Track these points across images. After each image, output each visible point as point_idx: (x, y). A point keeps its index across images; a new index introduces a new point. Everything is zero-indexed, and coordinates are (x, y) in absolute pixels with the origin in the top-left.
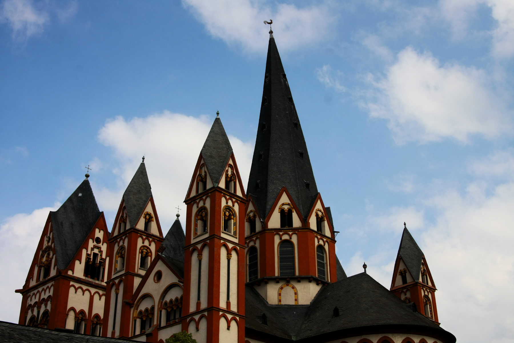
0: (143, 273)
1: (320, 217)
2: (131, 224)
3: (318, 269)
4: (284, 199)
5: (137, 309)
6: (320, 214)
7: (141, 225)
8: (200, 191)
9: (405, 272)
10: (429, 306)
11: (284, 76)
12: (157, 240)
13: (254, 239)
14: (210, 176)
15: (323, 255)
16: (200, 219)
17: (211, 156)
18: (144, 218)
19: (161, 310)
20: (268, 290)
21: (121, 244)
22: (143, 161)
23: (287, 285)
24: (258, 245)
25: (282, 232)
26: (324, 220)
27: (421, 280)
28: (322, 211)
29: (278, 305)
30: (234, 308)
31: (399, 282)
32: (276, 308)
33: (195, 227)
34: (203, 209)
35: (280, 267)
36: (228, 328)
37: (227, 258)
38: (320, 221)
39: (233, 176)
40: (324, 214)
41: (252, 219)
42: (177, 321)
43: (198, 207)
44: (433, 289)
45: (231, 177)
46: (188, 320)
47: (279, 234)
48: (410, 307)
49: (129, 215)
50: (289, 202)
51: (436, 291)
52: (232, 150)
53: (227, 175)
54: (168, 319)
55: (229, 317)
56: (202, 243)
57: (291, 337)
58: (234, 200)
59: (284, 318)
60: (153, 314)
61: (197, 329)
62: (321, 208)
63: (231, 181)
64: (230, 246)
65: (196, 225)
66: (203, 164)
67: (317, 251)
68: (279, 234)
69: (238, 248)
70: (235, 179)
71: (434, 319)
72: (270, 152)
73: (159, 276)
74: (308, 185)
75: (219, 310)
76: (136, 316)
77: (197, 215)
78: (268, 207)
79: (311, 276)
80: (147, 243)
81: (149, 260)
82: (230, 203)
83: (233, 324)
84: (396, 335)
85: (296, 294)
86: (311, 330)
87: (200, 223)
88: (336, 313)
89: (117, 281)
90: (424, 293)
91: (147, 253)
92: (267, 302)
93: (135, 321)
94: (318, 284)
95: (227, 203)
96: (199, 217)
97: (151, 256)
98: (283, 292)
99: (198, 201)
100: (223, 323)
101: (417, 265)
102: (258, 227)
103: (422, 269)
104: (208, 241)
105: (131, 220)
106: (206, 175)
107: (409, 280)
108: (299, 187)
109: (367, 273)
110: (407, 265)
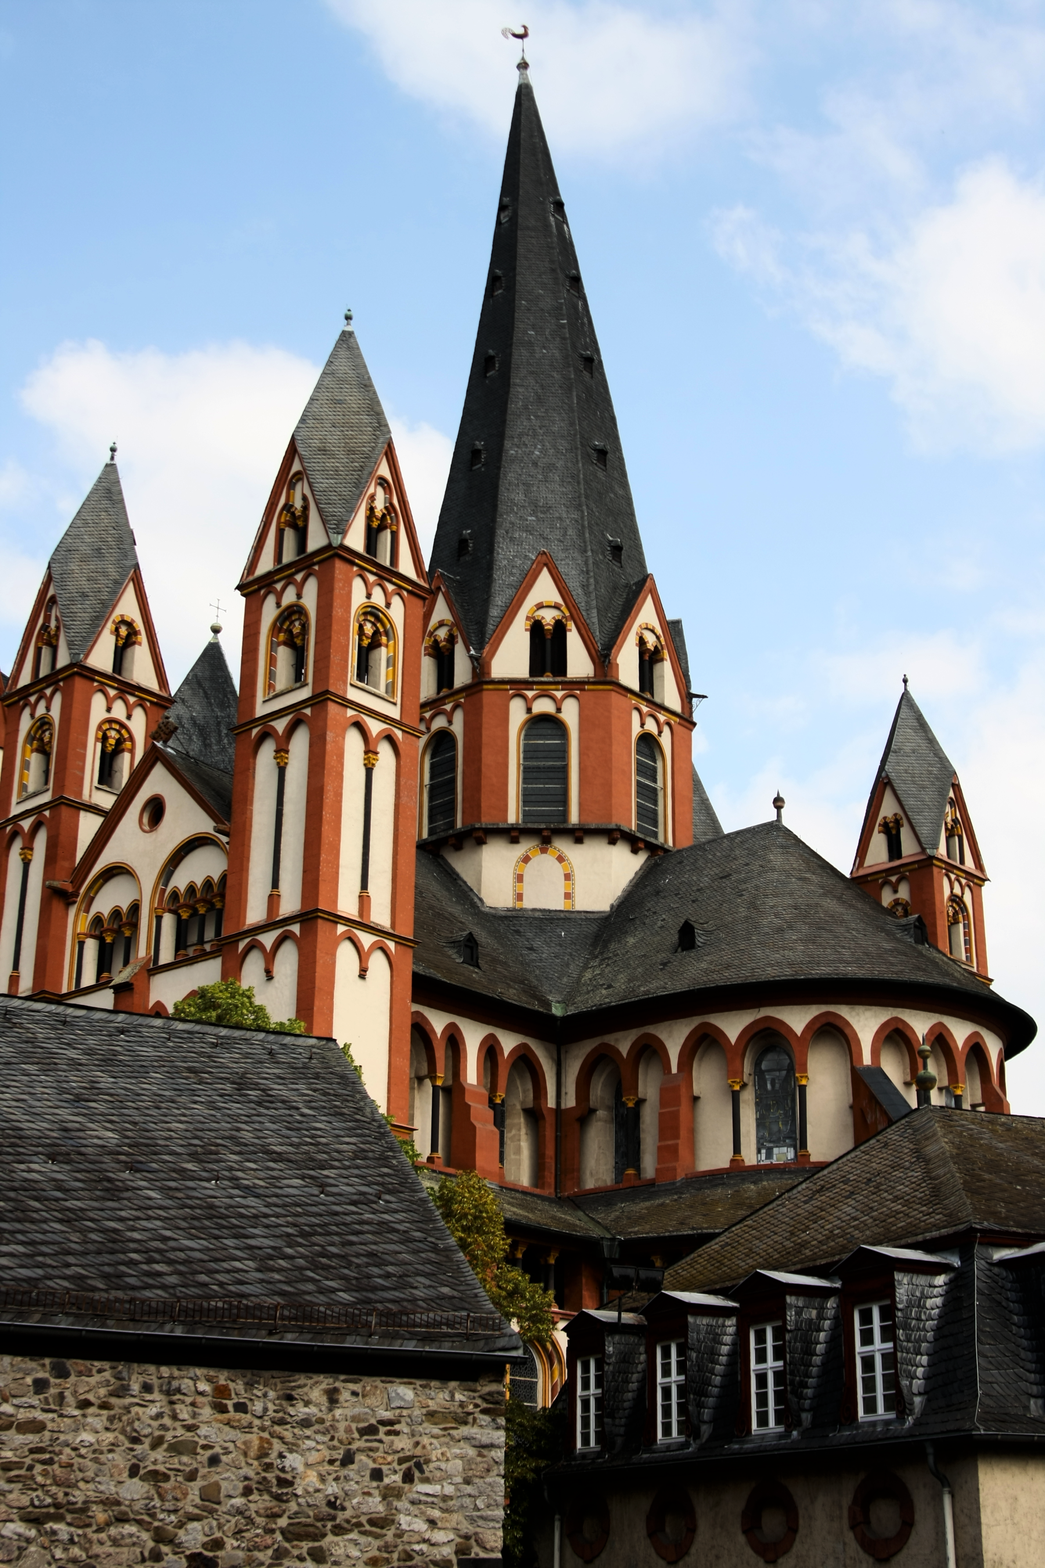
0: (106, 801)
1: (649, 650)
2: (73, 651)
5: (87, 911)
6: (651, 640)
7: (101, 658)
8: (288, 556)
9: (898, 823)
10: (964, 928)
11: (559, 206)
12: (151, 702)
13: (448, 707)
14: (320, 511)
15: (655, 763)
16: (285, 643)
17: (323, 450)
18: (112, 633)
19: (160, 914)
20: (484, 864)
21: (41, 710)
22: (112, 458)
23: (544, 851)
24: (457, 728)
25: (532, 689)
26: (662, 660)
27: (942, 850)
28: (659, 630)
29: (514, 909)
30: (381, 915)
31: (878, 854)
32: (506, 917)
33: (270, 666)
34: (294, 612)
35: (524, 795)
36: (362, 975)
37: (365, 765)
38: (648, 660)
39: (389, 514)
40: (662, 639)
41: (444, 646)
42: (207, 947)
43: (278, 605)
44: (977, 880)
45: (384, 515)
46: (242, 945)
47: (524, 697)
48: (906, 930)
49: (67, 623)
50: (560, 601)
51: (986, 883)
52: (389, 432)
53: (372, 509)
54: (180, 943)
55: (367, 939)
56: (290, 717)
57: (548, 1005)
58: (390, 587)
59: (531, 949)
60: (135, 926)
61: (269, 975)
62: (655, 623)
63: (382, 528)
64: (375, 727)
66: (298, 473)
67: (638, 752)
68: (524, 697)
69: (399, 734)
70: (395, 523)
71: (975, 965)
72: (506, 442)
73: (156, 810)
74: (617, 550)
76: (83, 931)
77: (276, 627)
78: (494, 612)
79: (614, 827)
80: (119, 711)
81: (125, 766)
82: (378, 598)
83: (378, 963)
84: (860, 1009)
85: (568, 877)
86: (610, 986)
87: (284, 654)
88: (687, 938)
89: (26, 824)
90: (952, 888)
91: (119, 742)
92: (481, 900)
93: (81, 944)
94: (635, 851)
95: (369, 596)
96: (282, 636)
97: (132, 751)
98: (529, 871)
99: (279, 586)
100: (346, 957)
101: (936, 803)
102: (462, 674)
103: (949, 819)
104: (308, 711)
105: (73, 639)
106: (306, 508)
107: (909, 847)
108: (589, 553)
109: (786, 822)
110: (904, 803)
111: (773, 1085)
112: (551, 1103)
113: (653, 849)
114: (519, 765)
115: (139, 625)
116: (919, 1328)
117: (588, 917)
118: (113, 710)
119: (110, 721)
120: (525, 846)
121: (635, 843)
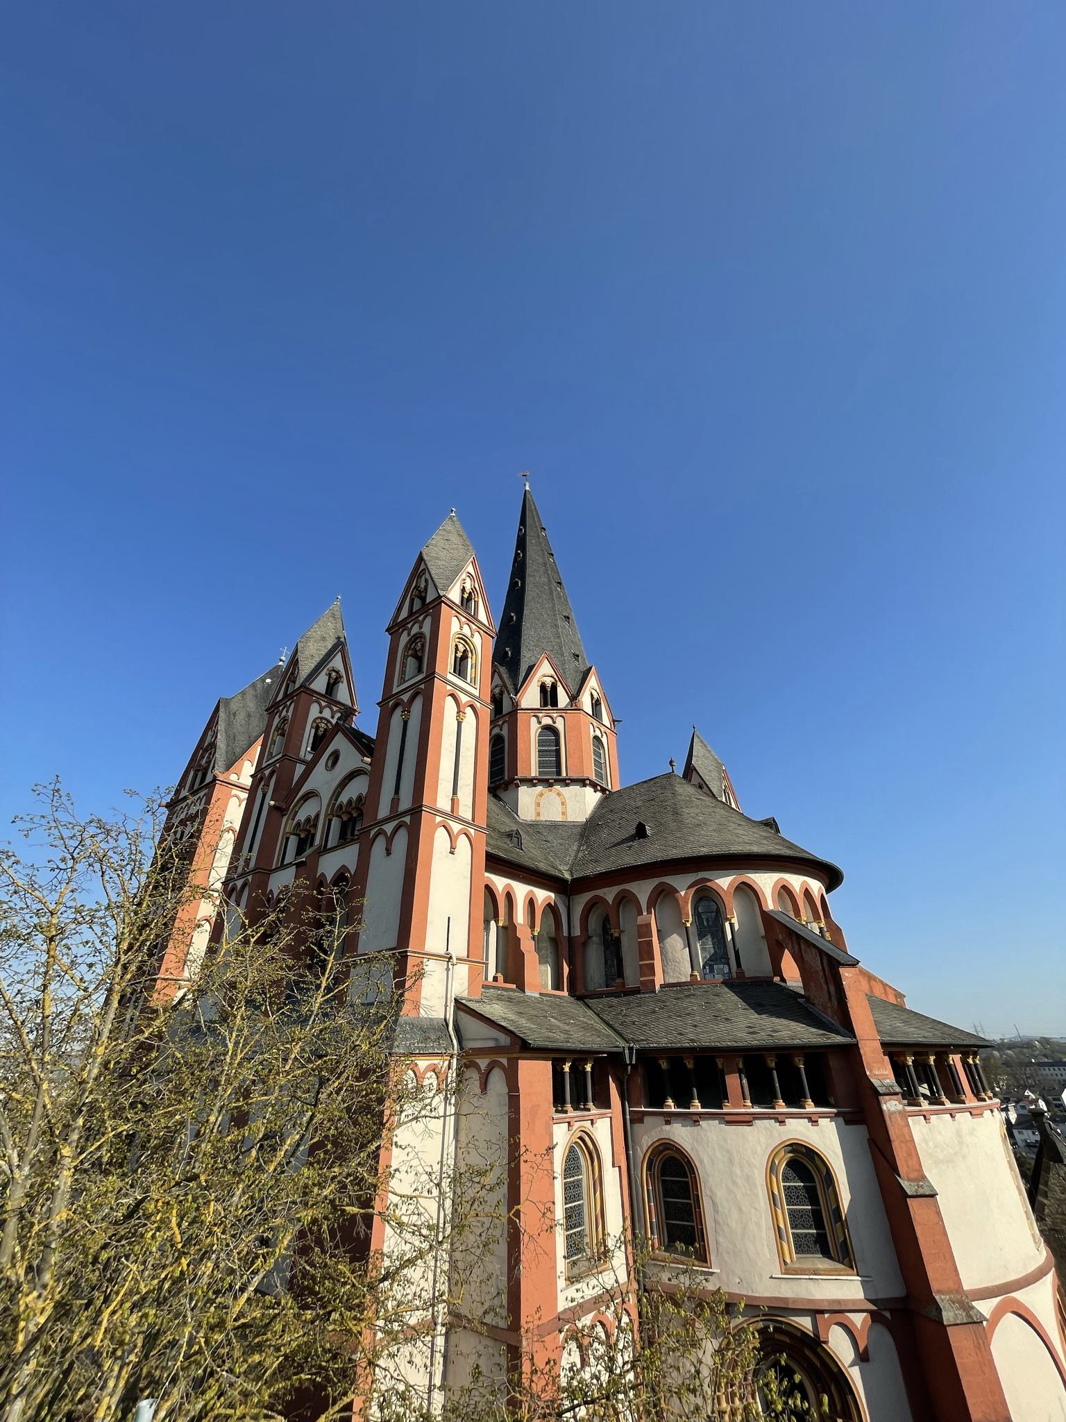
5: (293, 820)
6: (596, 696)
13: (500, 723)
16: (412, 656)
21: (284, 713)
30: (465, 812)
34: (417, 638)
35: (539, 764)
43: (409, 634)
46: (373, 833)
55: (456, 827)
60: (315, 826)
61: (388, 852)
64: (464, 699)
65: (404, 665)
66: (424, 570)
73: (336, 756)
77: (407, 648)
78: (521, 679)
82: (466, 630)
83: (463, 843)
85: (563, 804)
87: (411, 662)
88: (640, 832)
93: (288, 839)
95: (461, 628)
98: (542, 801)
100: (441, 837)
111: (707, 920)
112: (565, 933)
113: (603, 790)
115: (343, 672)
117: (574, 825)
119: (322, 718)
120: (539, 788)
121: (594, 786)
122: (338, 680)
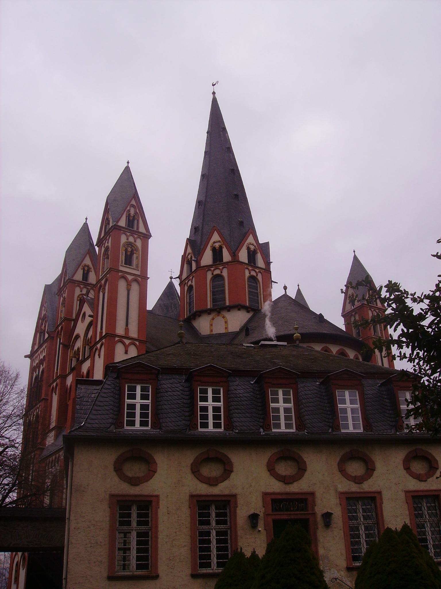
3: (249, 298)
4: (216, 237)
6: (252, 248)
13: (191, 278)
18: (81, 269)
22: (86, 221)
24: (193, 284)
25: (213, 268)
28: (255, 244)
37: (127, 289)
55: (127, 342)
58: (136, 236)
62: (253, 242)
64: (130, 278)
67: (248, 281)
71: (384, 337)
75: (115, 336)
82: (131, 239)
85: (226, 322)
93: (72, 360)
94: (248, 312)
95: (128, 239)
114: (210, 291)
115: (91, 266)
116: (87, 404)
118: (83, 291)
121: (248, 309)
122: (89, 271)
